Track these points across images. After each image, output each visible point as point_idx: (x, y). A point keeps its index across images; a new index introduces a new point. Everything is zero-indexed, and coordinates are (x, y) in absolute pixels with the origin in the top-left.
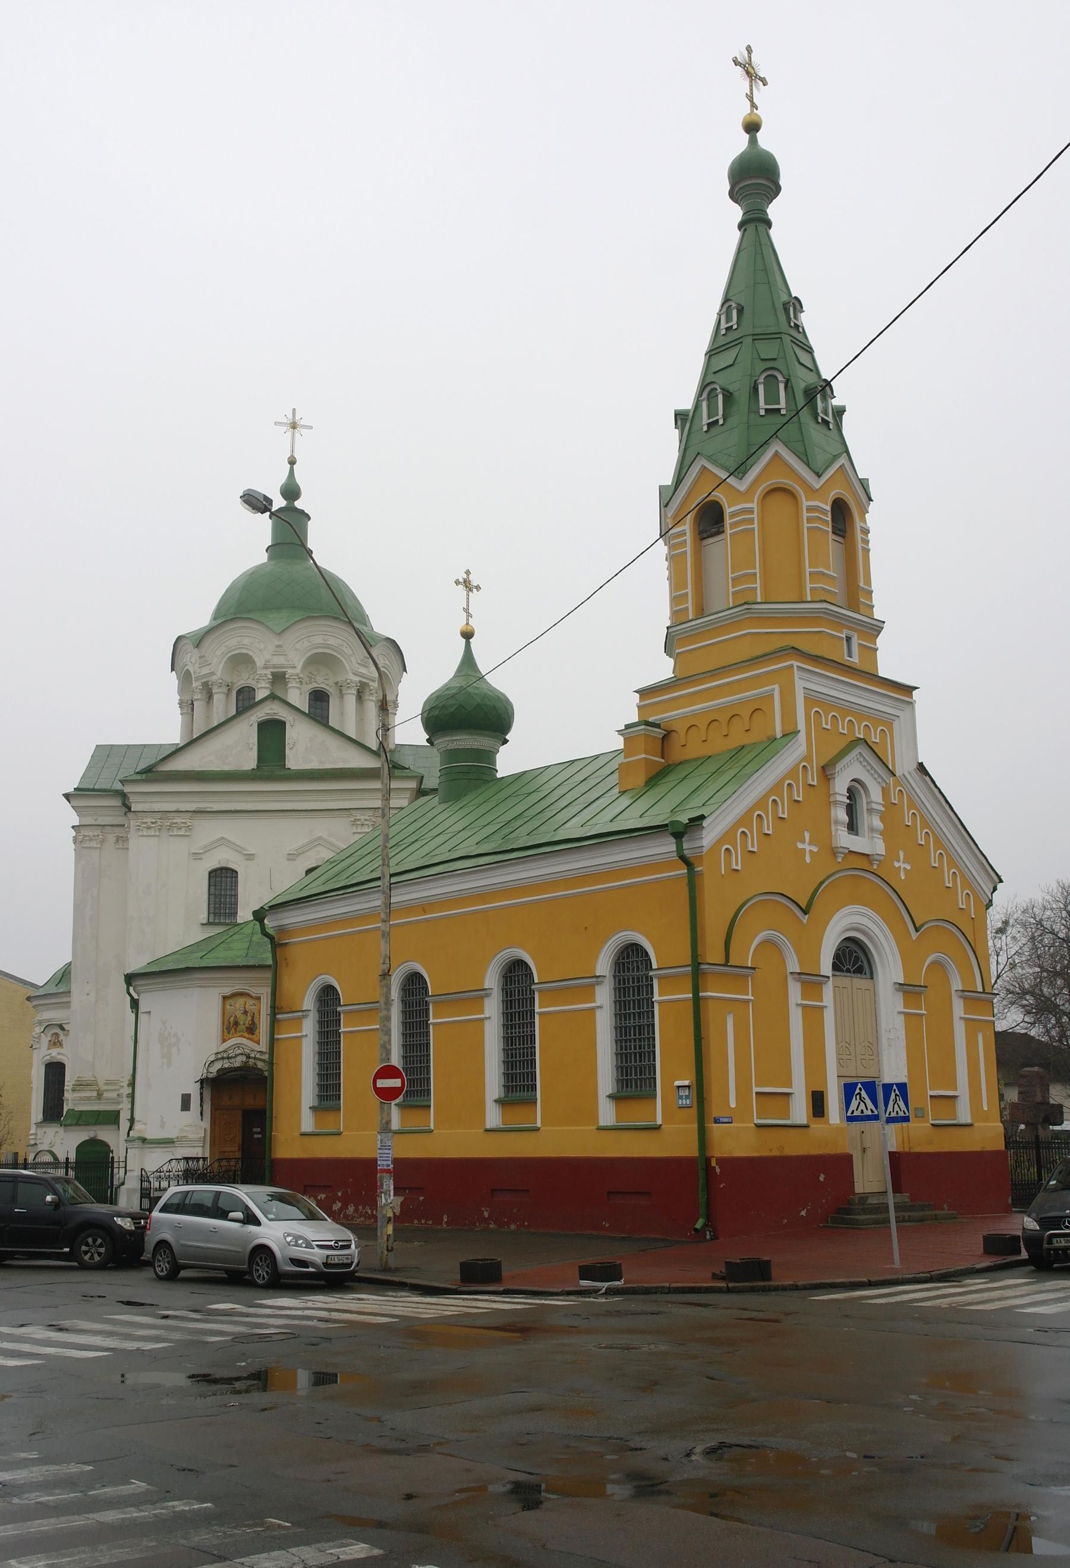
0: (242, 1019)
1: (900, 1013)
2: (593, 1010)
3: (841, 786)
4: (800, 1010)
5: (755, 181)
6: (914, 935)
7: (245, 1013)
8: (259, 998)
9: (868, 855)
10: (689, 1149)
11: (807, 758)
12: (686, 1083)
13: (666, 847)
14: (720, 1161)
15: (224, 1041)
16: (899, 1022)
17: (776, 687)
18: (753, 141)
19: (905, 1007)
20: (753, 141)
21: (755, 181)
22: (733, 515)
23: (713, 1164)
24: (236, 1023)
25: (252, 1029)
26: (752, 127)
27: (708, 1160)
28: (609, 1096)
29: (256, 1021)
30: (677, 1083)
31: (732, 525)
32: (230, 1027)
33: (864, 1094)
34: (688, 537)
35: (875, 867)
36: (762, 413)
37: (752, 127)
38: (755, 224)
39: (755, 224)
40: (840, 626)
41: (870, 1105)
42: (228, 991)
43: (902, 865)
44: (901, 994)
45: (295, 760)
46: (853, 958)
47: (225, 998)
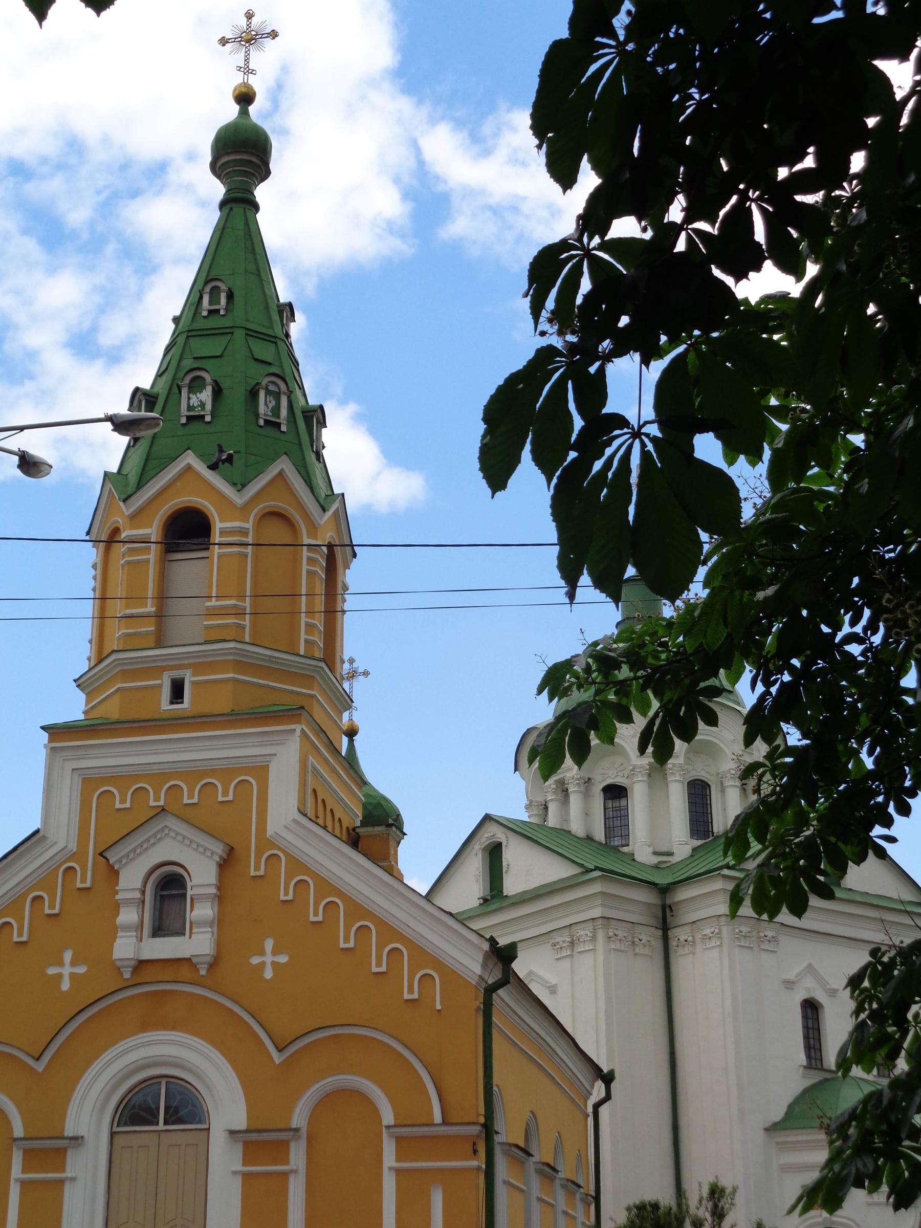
1: (235, 1173)
3: (132, 878)
4: (18, 1186)
6: (277, 1058)
9: (188, 960)
11: (79, 855)
16: (236, 1186)
18: (244, 113)
19: (245, 1163)
20: (244, 113)
26: (245, 98)
35: (203, 972)
37: (245, 98)
38: (239, 205)
39: (239, 205)
40: (157, 671)
43: (269, 959)
44: (239, 1148)
45: (512, 886)
46: (162, 1106)
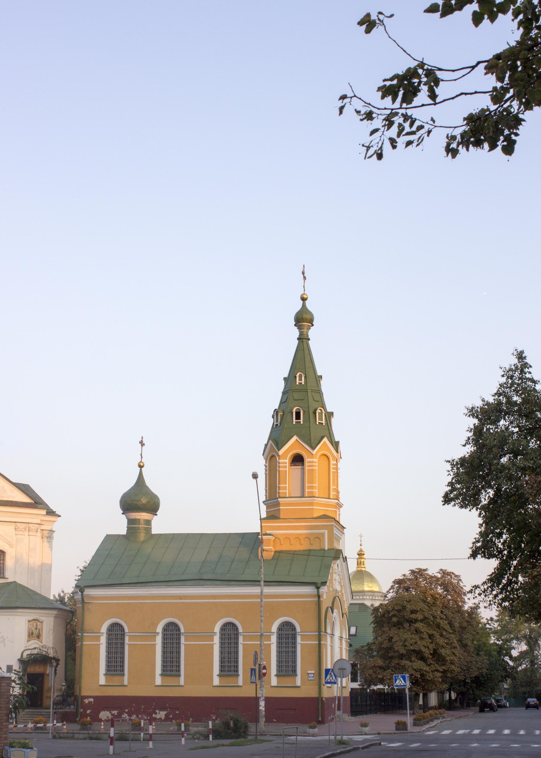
0: (35, 631)
2: (270, 644)
5: (303, 319)
7: (36, 629)
8: (42, 622)
10: (314, 694)
12: (313, 672)
13: (309, 590)
14: (326, 698)
15: (28, 641)
17: (326, 531)
21: (303, 319)
22: (308, 462)
23: (324, 699)
24: (32, 633)
25: (39, 637)
27: (322, 698)
28: (275, 675)
29: (40, 633)
30: (309, 672)
31: (308, 466)
32: (31, 635)
33: (401, 679)
34: (287, 465)
36: (317, 423)
41: (403, 682)
42: (31, 618)
47: (29, 621)
